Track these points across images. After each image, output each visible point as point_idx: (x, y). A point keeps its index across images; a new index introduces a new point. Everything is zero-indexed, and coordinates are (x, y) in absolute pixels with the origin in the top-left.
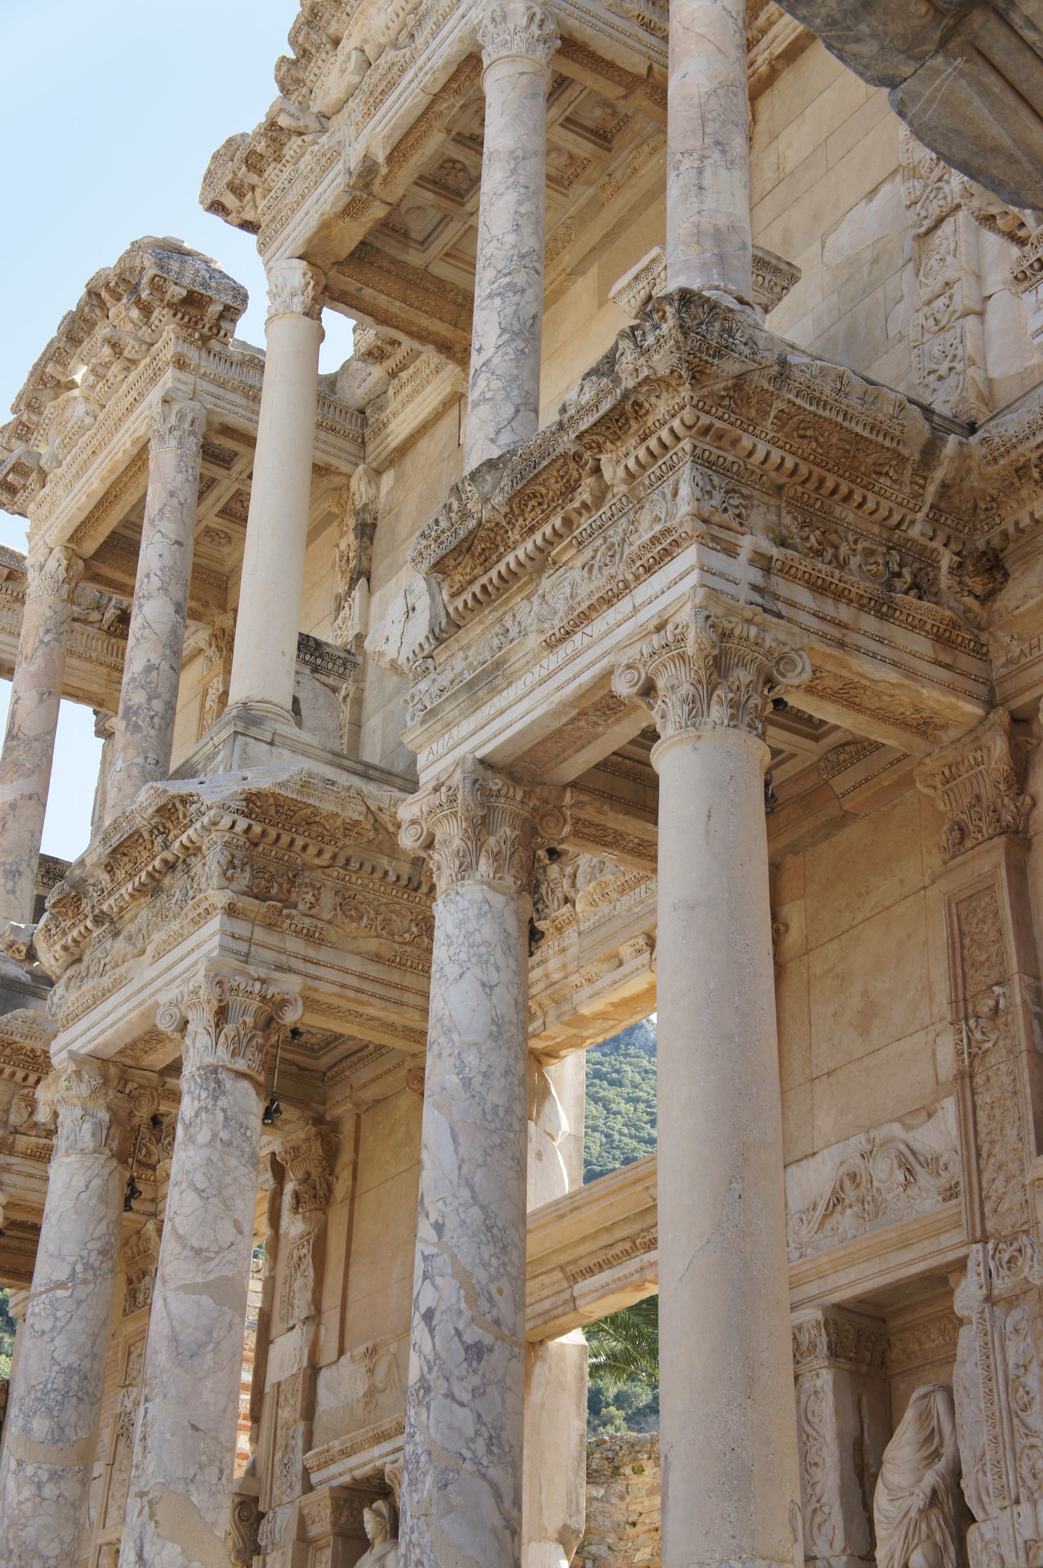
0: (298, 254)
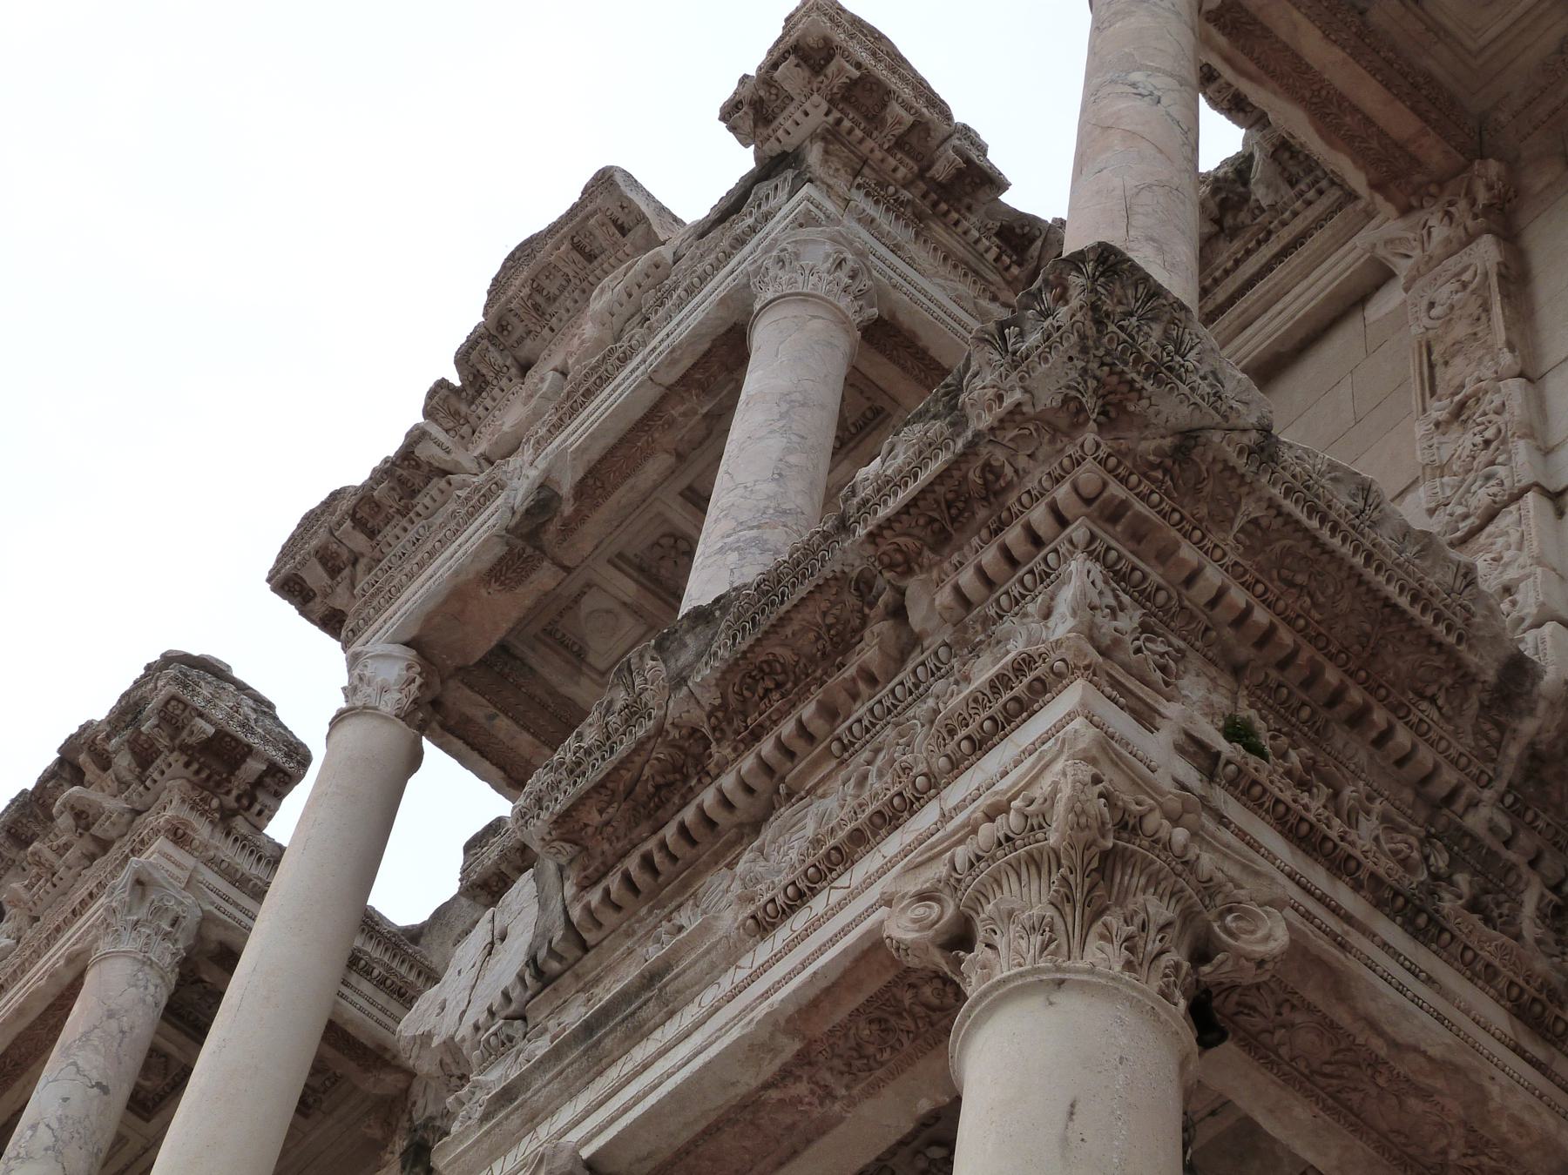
0: (407, 637)
